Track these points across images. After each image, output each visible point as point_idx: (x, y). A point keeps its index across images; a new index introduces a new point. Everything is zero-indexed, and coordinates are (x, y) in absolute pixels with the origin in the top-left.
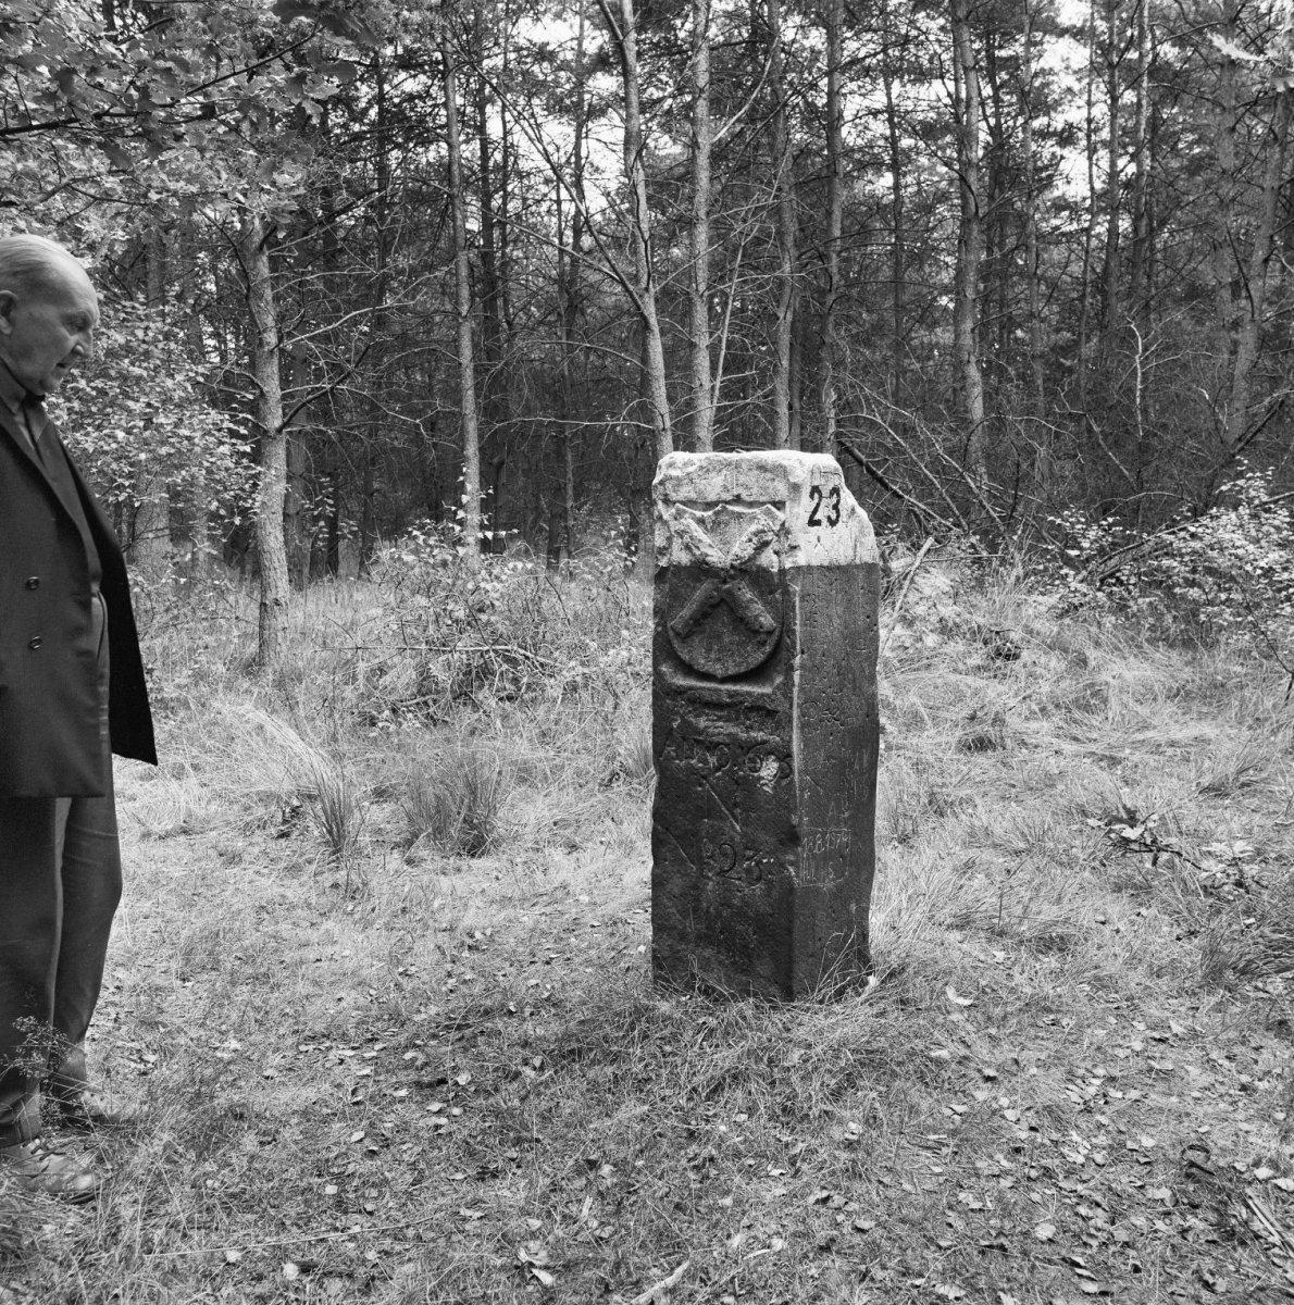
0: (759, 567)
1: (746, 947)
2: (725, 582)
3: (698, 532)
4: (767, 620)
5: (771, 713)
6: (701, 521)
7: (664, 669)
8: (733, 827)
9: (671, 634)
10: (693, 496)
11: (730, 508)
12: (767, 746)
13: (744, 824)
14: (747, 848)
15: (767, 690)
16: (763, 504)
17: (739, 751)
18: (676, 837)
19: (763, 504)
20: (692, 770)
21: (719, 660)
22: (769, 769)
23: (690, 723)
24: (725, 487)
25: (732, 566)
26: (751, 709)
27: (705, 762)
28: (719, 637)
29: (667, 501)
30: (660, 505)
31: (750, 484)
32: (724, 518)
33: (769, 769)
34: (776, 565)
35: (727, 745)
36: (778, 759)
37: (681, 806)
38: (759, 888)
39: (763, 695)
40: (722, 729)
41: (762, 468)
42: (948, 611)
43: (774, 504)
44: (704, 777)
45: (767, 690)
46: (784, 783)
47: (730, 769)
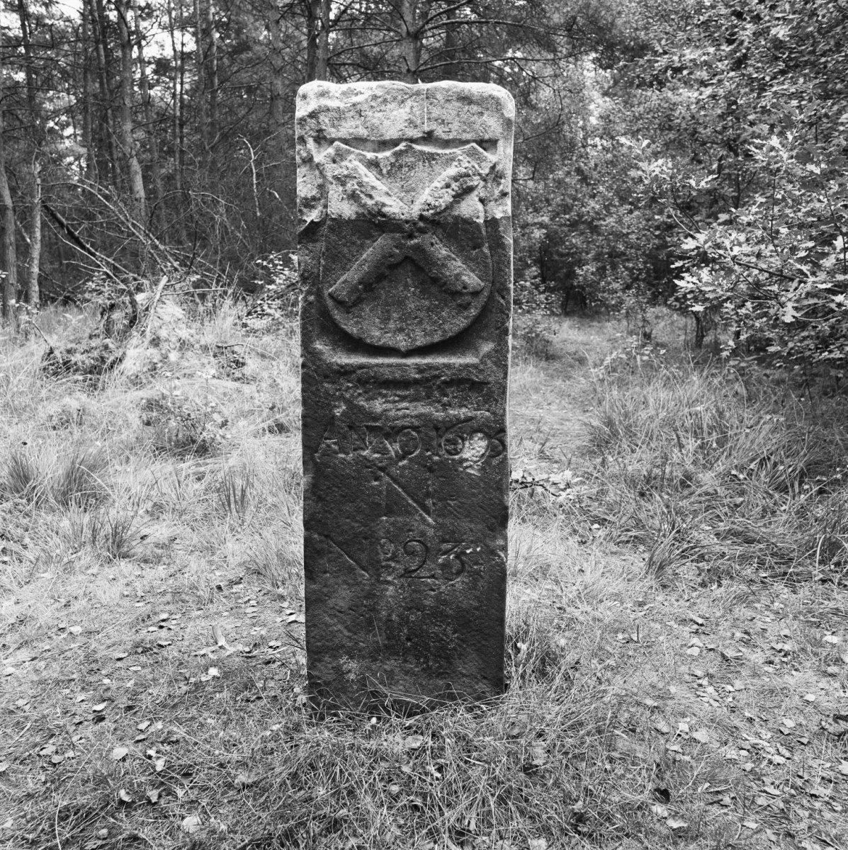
0: (457, 218)
1: (443, 648)
2: (411, 236)
3: (370, 177)
4: (471, 279)
5: (477, 386)
6: (373, 165)
7: (319, 346)
8: (424, 520)
9: (330, 303)
10: (363, 132)
11: (417, 147)
12: (474, 424)
13: (441, 514)
14: (444, 541)
15: (470, 359)
16: (467, 142)
17: (433, 433)
18: (339, 544)
19: (467, 142)
20: (366, 463)
21: (401, 330)
22: (475, 449)
23: (361, 409)
24: (411, 122)
25: (421, 217)
26: (448, 384)
27: (384, 451)
28: (401, 303)
29: (321, 139)
30: (311, 144)
31: (449, 118)
32: (410, 159)
33: (475, 449)
34: (482, 214)
35: (415, 428)
36: (488, 436)
37: (348, 507)
38: (459, 582)
39: (467, 366)
40: (408, 410)
41: (466, 99)
42: (184, 333)
43: (481, 142)
44: (382, 469)
45: (470, 359)
46: (495, 462)
47: (421, 455)
